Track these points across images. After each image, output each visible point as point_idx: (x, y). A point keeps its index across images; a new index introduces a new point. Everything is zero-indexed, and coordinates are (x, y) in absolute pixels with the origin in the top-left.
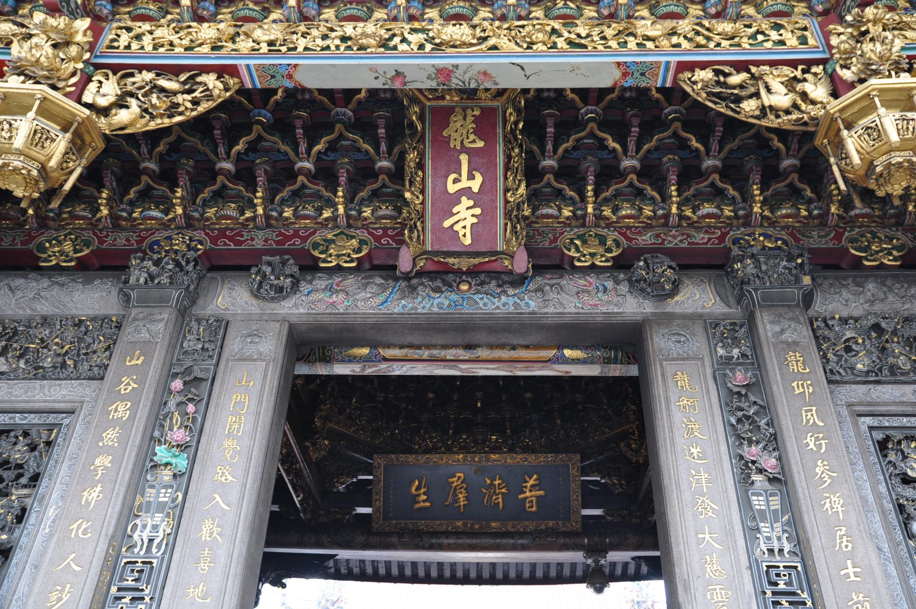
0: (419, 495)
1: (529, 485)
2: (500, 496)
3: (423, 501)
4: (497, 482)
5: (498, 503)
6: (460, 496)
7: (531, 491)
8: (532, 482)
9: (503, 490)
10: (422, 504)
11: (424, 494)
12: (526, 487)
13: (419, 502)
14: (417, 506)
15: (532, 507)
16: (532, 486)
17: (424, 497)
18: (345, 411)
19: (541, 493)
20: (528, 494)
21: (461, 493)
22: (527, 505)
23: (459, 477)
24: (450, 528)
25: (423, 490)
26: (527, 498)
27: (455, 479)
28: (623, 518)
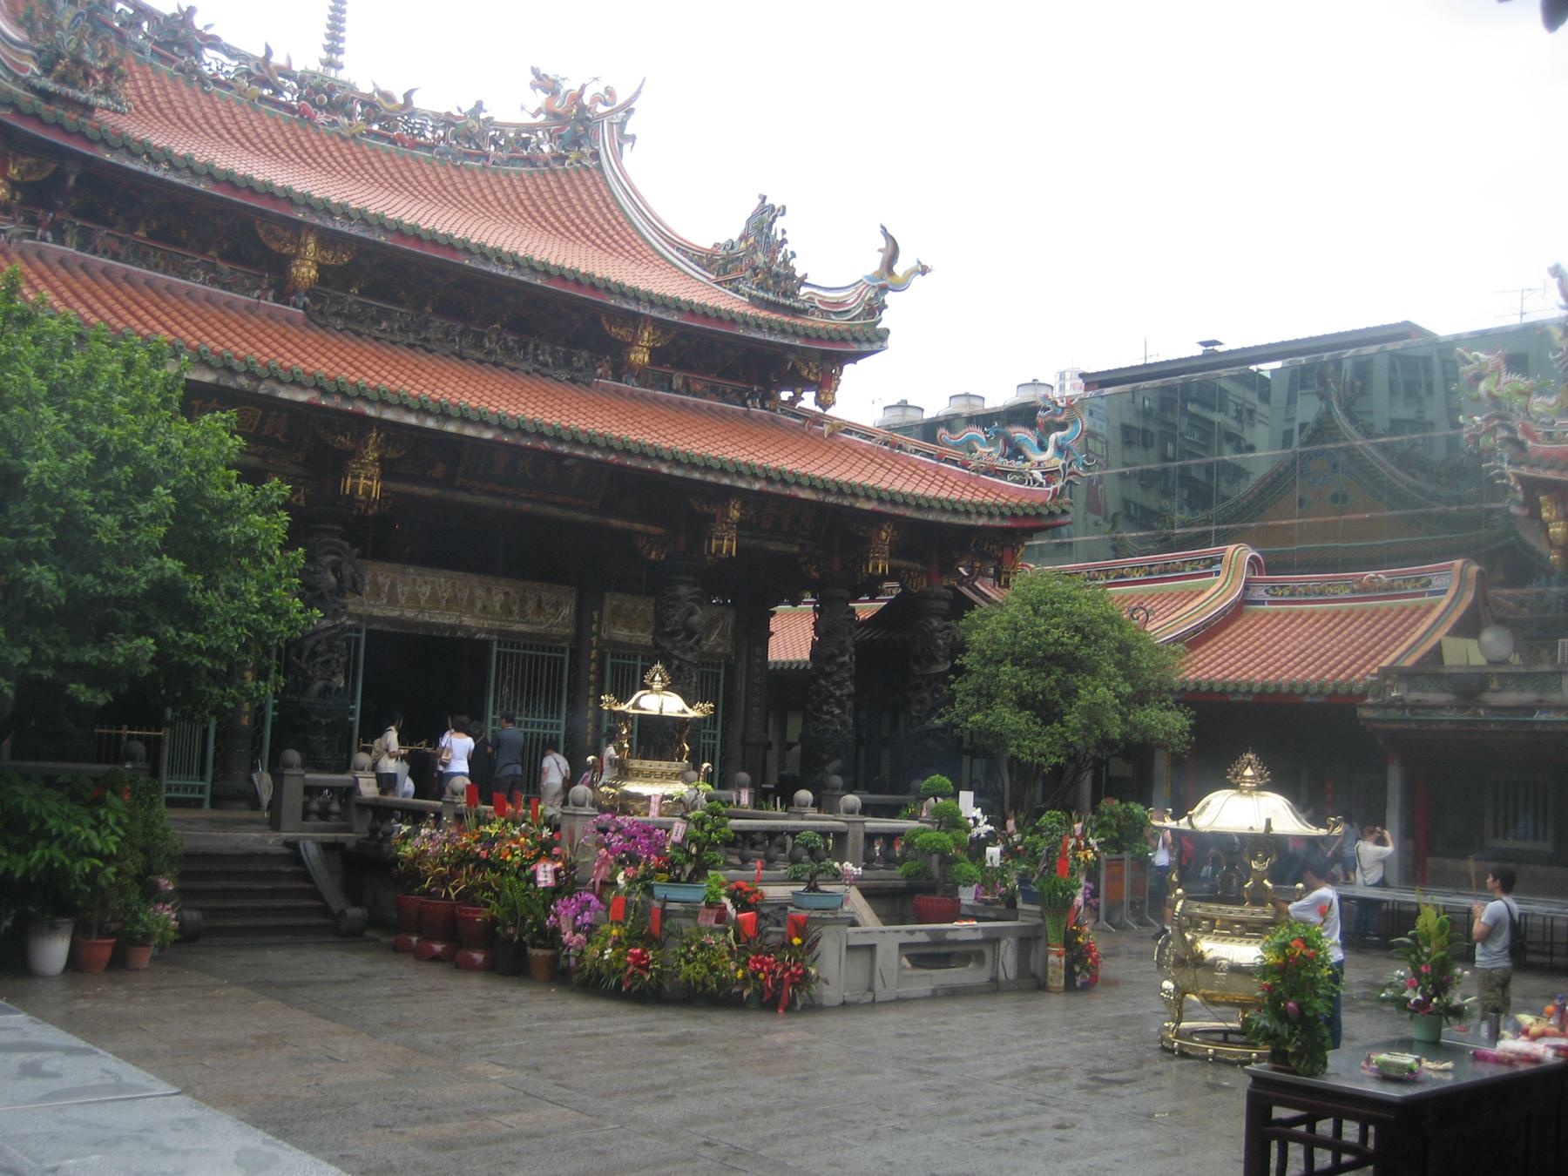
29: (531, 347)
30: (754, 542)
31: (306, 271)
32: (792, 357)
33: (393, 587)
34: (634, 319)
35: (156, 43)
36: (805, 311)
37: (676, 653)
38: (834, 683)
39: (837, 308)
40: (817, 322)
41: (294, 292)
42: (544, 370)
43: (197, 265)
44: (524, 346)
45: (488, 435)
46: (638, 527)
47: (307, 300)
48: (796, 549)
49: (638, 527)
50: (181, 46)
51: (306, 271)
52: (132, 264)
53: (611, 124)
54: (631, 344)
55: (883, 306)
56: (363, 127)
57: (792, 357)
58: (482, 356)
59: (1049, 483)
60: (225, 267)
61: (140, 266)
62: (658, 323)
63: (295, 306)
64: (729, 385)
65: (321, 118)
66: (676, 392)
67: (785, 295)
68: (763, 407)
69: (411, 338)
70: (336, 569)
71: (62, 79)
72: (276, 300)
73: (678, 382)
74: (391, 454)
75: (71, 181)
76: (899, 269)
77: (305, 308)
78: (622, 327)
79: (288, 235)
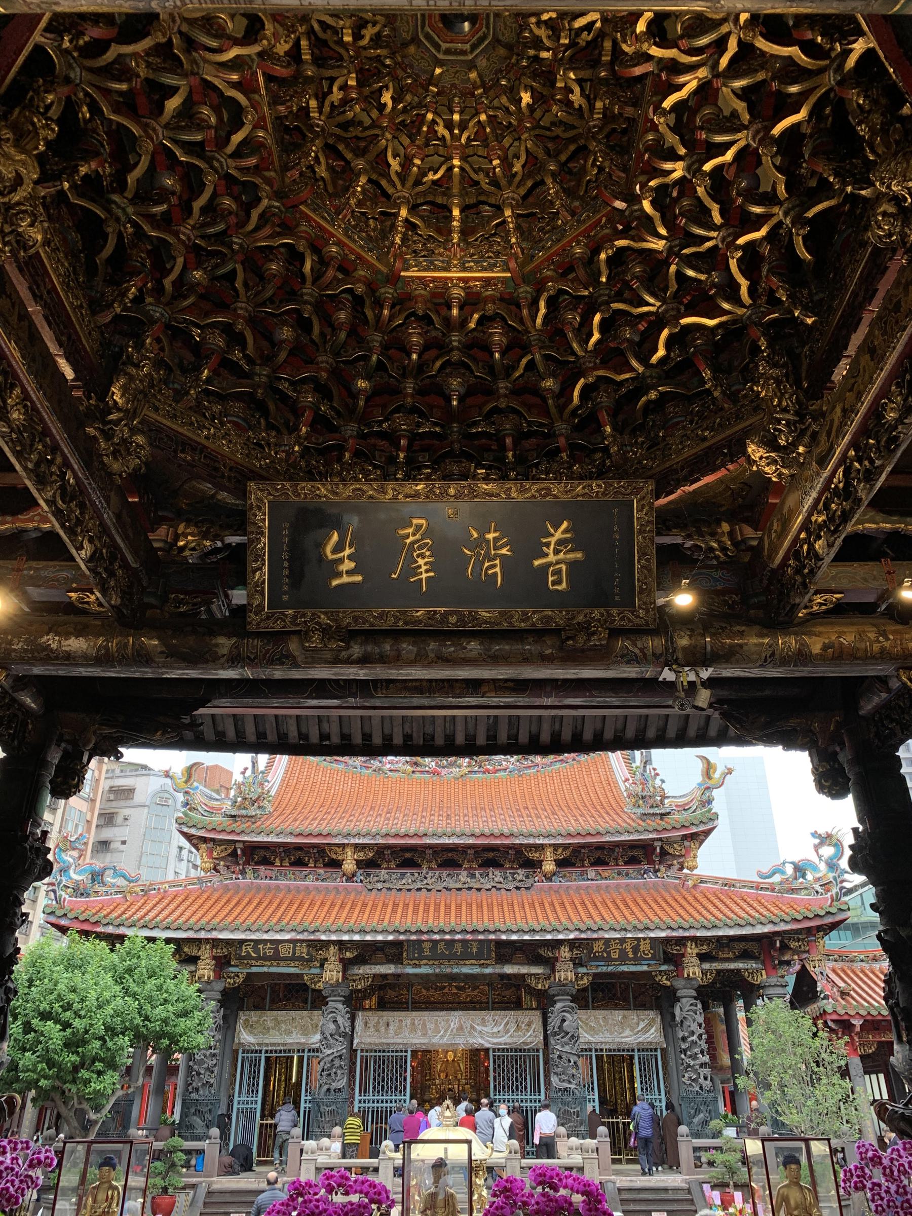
0: (341, 561)
1: (553, 540)
2: (497, 562)
3: (350, 573)
4: (490, 536)
5: (495, 574)
6: (421, 561)
7: (556, 552)
8: (558, 535)
9: (504, 551)
10: (345, 579)
11: (350, 557)
12: (548, 545)
13: (339, 575)
14: (335, 583)
15: (559, 582)
16: (560, 542)
17: (348, 565)
18: (187, 393)
19: (579, 555)
20: (552, 558)
21: (422, 556)
22: (550, 579)
23: (419, 527)
24: (401, 623)
25: (348, 552)
26: (550, 564)
27: (411, 530)
28: (731, 607)
30: (610, 968)
31: (349, 866)
32: (658, 844)
33: (424, 1025)
34: (541, 848)
36: (669, 813)
37: (558, 1047)
38: (690, 1057)
39: (684, 808)
40: (677, 817)
41: (354, 876)
42: (499, 886)
43: (310, 873)
45: (391, 938)
46: (524, 970)
48: (645, 968)
49: (524, 970)
51: (349, 866)
55: (710, 802)
56: (466, 770)
57: (659, 844)
58: (459, 886)
59: (828, 891)
60: (321, 871)
62: (555, 847)
64: (631, 869)
65: (444, 772)
67: (652, 807)
68: (657, 877)
69: (419, 885)
70: (335, 1021)
71: (239, 808)
74: (348, 955)
75: (239, 852)
76: (717, 775)
77: (361, 881)
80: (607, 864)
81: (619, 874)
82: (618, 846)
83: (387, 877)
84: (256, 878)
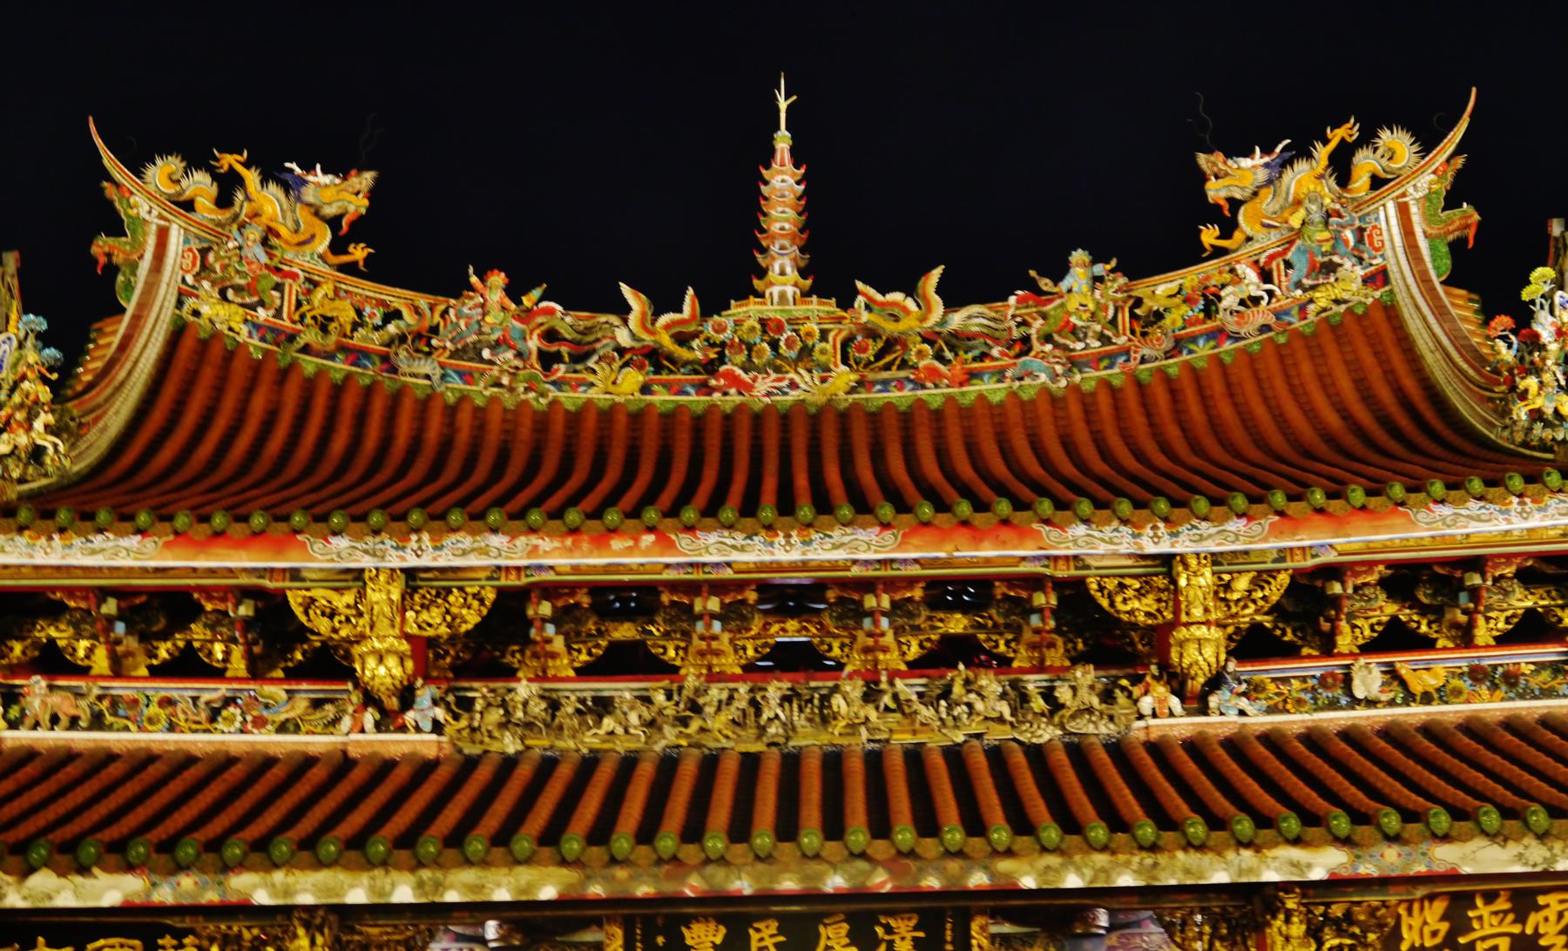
29: (958, 689)
35: (455, 354)
43: (229, 701)
44: (946, 693)
47: (440, 713)
50: (495, 346)
52: (110, 728)
53: (1403, 210)
54: (1175, 624)
61: (127, 729)
63: (418, 729)
66: (1371, 703)
72: (379, 727)
73: (1368, 678)
77: (437, 727)
78: (1140, 594)
79: (349, 598)
80: (1427, 644)
81: (1477, 674)
82: (1476, 564)
83: (538, 708)
84: (13, 725)
